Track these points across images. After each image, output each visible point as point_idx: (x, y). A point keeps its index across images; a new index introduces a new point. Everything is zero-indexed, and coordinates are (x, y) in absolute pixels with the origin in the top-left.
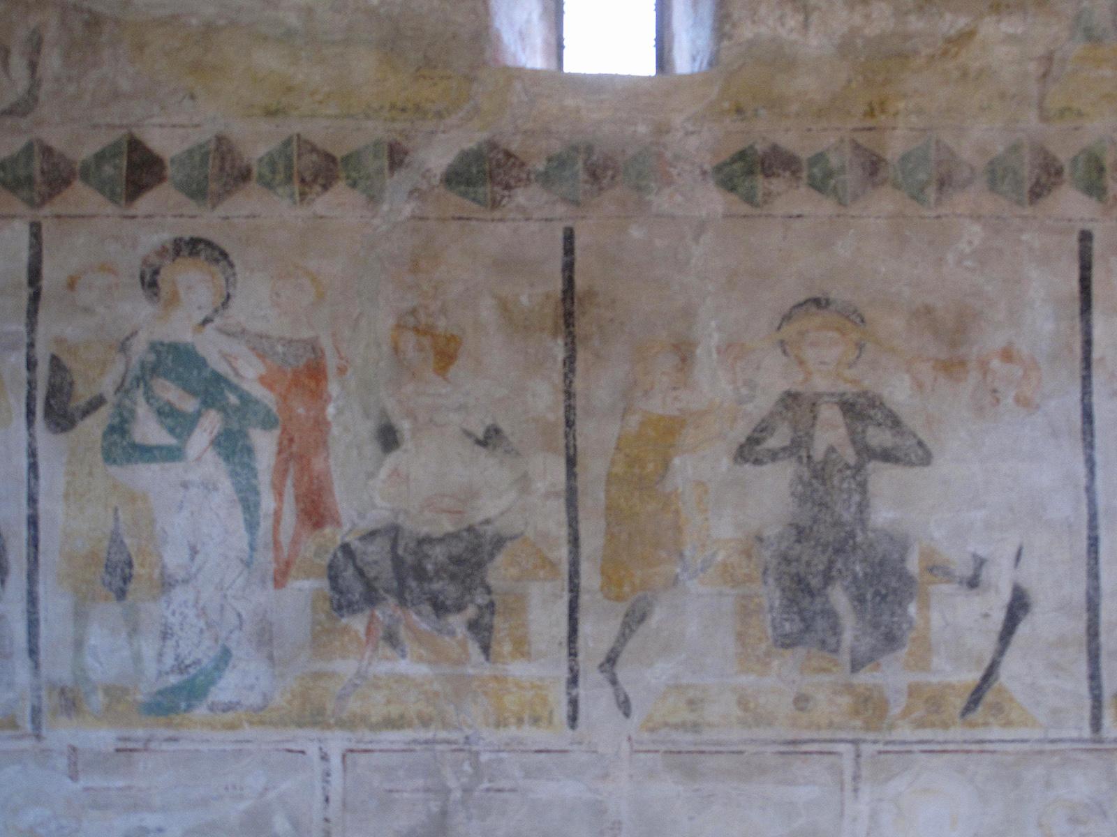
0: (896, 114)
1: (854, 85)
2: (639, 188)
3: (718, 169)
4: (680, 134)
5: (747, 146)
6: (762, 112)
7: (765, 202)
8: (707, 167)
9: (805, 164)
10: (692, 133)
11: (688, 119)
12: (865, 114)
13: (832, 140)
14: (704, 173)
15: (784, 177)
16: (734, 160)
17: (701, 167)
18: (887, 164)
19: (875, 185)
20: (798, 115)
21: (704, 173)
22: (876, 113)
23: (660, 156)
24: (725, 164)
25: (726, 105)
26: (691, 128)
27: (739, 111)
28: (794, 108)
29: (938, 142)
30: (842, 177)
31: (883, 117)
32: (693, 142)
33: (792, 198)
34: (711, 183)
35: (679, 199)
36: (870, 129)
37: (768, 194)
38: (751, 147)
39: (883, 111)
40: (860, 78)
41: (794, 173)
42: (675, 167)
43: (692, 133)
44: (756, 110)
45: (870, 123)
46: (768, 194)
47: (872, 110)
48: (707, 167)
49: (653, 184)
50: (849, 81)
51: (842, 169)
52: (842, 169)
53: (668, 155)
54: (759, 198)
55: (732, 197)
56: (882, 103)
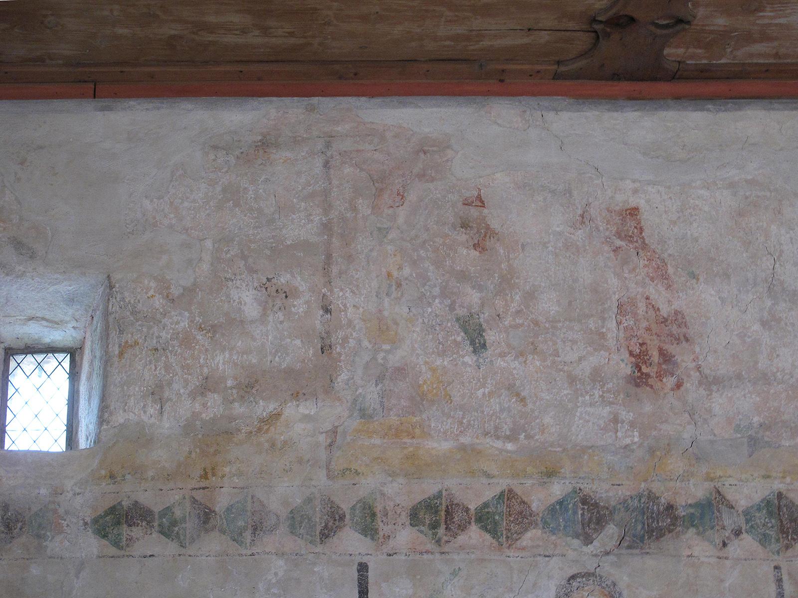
0: (223, 476)
1: (193, 455)
2: (39, 536)
3: (95, 521)
4: (70, 495)
5: (116, 503)
6: (128, 477)
7: (128, 545)
8: (88, 520)
9: (157, 517)
10: (78, 494)
11: (76, 484)
12: (201, 477)
13: (177, 497)
14: (86, 524)
15: (141, 526)
16: (107, 513)
17: (84, 520)
18: (216, 514)
19: (207, 531)
20: (153, 479)
21: (86, 524)
22: (210, 475)
23: (55, 511)
24: (101, 517)
25: (103, 472)
26: (78, 490)
27: (112, 477)
28: (150, 473)
29: (253, 497)
30: (183, 525)
31: (214, 479)
32: (79, 500)
33: (147, 542)
34: (90, 533)
35: (67, 543)
36: (204, 488)
37: (130, 539)
38: (120, 503)
39: (214, 475)
40: (198, 450)
41: (148, 523)
42: (65, 520)
43: (78, 494)
44: (124, 476)
45: (202, 485)
46: (130, 539)
47: (206, 473)
48: (88, 520)
49: (48, 534)
50: (190, 453)
51: (184, 520)
52: (184, 520)
53: (61, 511)
54: (124, 543)
55: (104, 542)
56: (213, 469)
